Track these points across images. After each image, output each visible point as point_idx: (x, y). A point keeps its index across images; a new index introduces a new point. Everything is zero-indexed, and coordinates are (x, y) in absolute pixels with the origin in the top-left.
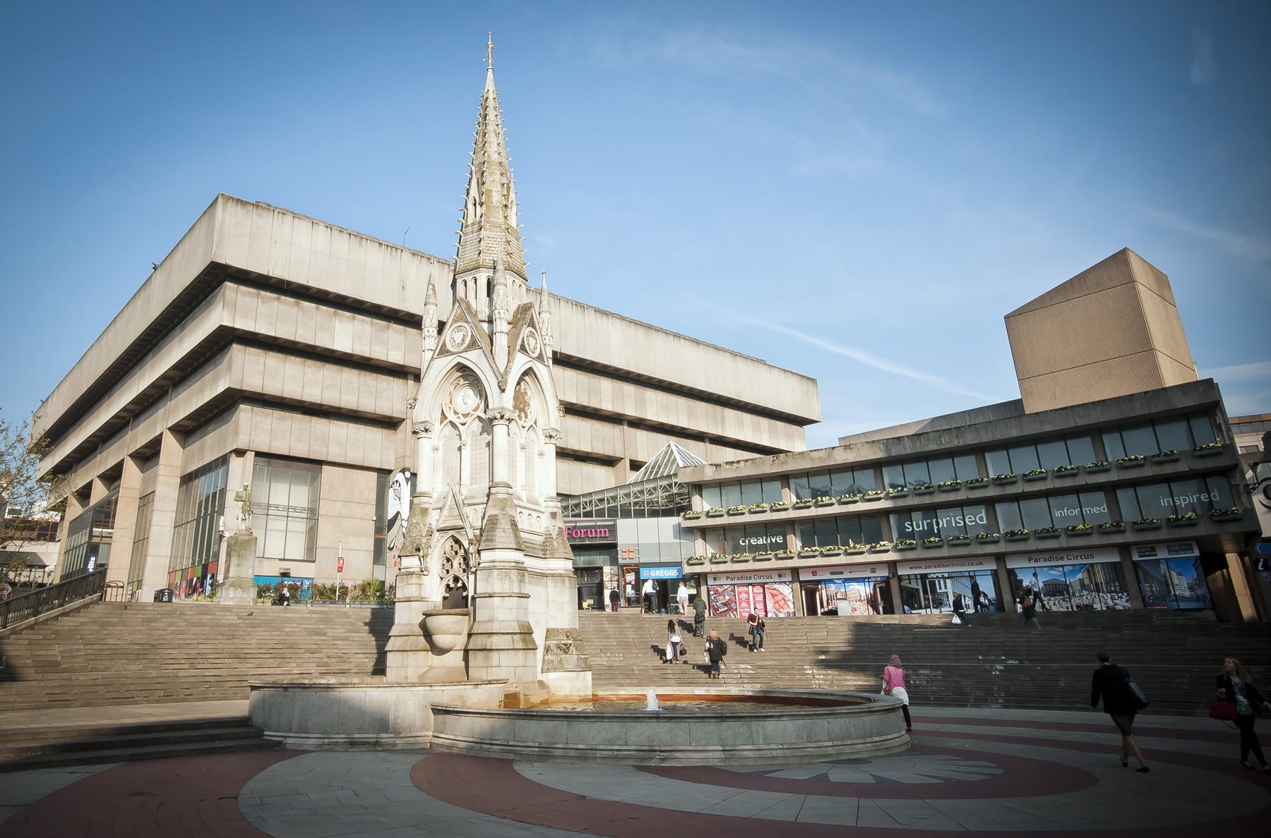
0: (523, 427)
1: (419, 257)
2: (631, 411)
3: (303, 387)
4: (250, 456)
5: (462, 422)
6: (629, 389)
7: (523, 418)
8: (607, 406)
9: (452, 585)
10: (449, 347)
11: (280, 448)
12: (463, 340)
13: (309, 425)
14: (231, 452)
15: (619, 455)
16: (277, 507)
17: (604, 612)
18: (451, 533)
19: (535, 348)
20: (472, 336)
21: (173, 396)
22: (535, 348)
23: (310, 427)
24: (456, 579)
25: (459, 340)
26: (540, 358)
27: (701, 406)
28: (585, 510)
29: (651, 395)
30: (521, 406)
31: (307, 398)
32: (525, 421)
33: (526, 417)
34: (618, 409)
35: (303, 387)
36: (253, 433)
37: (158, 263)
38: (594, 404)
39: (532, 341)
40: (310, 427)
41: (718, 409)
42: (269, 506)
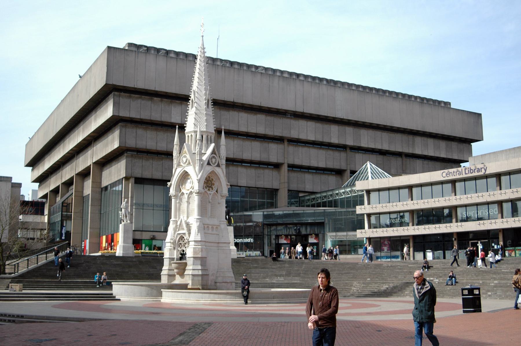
0: (210, 194)
1: (217, 66)
2: (350, 142)
3: (157, 143)
4: (132, 181)
5: (187, 193)
6: (349, 130)
7: (211, 190)
8: (335, 140)
9: (182, 253)
10: (182, 164)
11: (147, 175)
12: (186, 161)
13: (161, 162)
14: (123, 178)
15: (343, 167)
16: (148, 205)
17: (320, 260)
18: (181, 235)
19: (215, 162)
20: (189, 160)
21: (94, 146)
22: (215, 162)
23: (162, 163)
24: (183, 251)
25: (185, 161)
26: (218, 166)
27: (398, 137)
28: (317, 202)
29: (364, 132)
30: (210, 185)
31: (159, 149)
32: (212, 191)
33: (212, 189)
34: (342, 142)
35: (157, 143)
36: (133, 168)
37: (81, 75)
38: (326, 140)
39: (214, 160)
40: (162, 163)
41: (411, 137)
42: (143, 205)
